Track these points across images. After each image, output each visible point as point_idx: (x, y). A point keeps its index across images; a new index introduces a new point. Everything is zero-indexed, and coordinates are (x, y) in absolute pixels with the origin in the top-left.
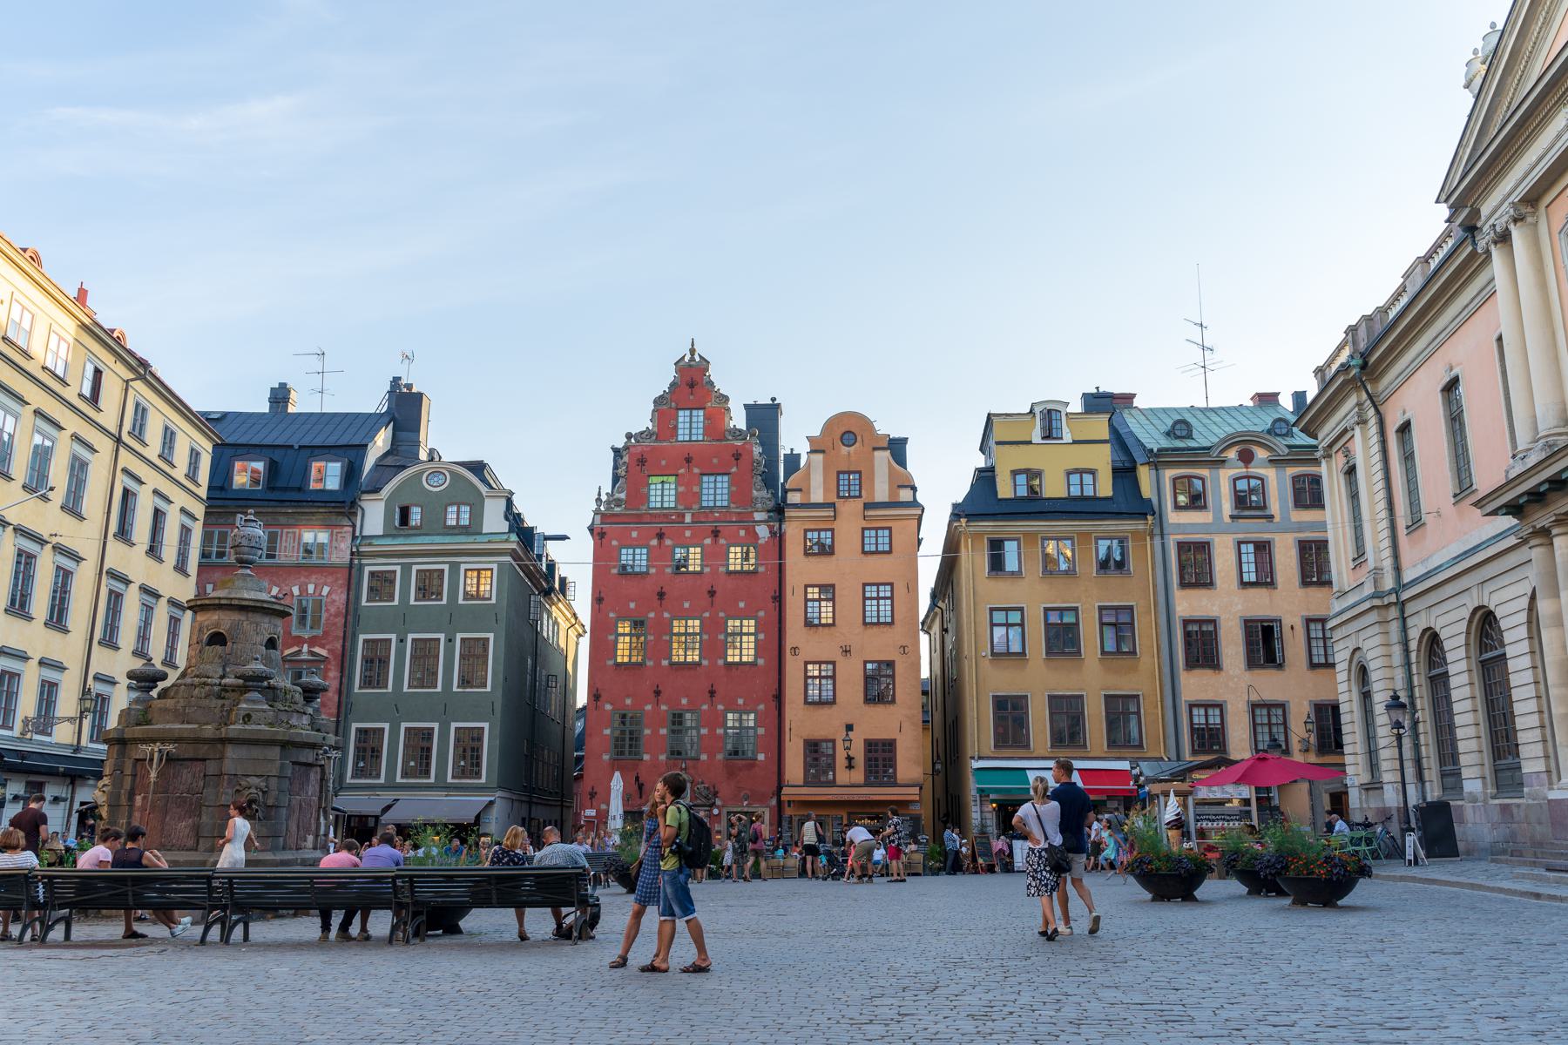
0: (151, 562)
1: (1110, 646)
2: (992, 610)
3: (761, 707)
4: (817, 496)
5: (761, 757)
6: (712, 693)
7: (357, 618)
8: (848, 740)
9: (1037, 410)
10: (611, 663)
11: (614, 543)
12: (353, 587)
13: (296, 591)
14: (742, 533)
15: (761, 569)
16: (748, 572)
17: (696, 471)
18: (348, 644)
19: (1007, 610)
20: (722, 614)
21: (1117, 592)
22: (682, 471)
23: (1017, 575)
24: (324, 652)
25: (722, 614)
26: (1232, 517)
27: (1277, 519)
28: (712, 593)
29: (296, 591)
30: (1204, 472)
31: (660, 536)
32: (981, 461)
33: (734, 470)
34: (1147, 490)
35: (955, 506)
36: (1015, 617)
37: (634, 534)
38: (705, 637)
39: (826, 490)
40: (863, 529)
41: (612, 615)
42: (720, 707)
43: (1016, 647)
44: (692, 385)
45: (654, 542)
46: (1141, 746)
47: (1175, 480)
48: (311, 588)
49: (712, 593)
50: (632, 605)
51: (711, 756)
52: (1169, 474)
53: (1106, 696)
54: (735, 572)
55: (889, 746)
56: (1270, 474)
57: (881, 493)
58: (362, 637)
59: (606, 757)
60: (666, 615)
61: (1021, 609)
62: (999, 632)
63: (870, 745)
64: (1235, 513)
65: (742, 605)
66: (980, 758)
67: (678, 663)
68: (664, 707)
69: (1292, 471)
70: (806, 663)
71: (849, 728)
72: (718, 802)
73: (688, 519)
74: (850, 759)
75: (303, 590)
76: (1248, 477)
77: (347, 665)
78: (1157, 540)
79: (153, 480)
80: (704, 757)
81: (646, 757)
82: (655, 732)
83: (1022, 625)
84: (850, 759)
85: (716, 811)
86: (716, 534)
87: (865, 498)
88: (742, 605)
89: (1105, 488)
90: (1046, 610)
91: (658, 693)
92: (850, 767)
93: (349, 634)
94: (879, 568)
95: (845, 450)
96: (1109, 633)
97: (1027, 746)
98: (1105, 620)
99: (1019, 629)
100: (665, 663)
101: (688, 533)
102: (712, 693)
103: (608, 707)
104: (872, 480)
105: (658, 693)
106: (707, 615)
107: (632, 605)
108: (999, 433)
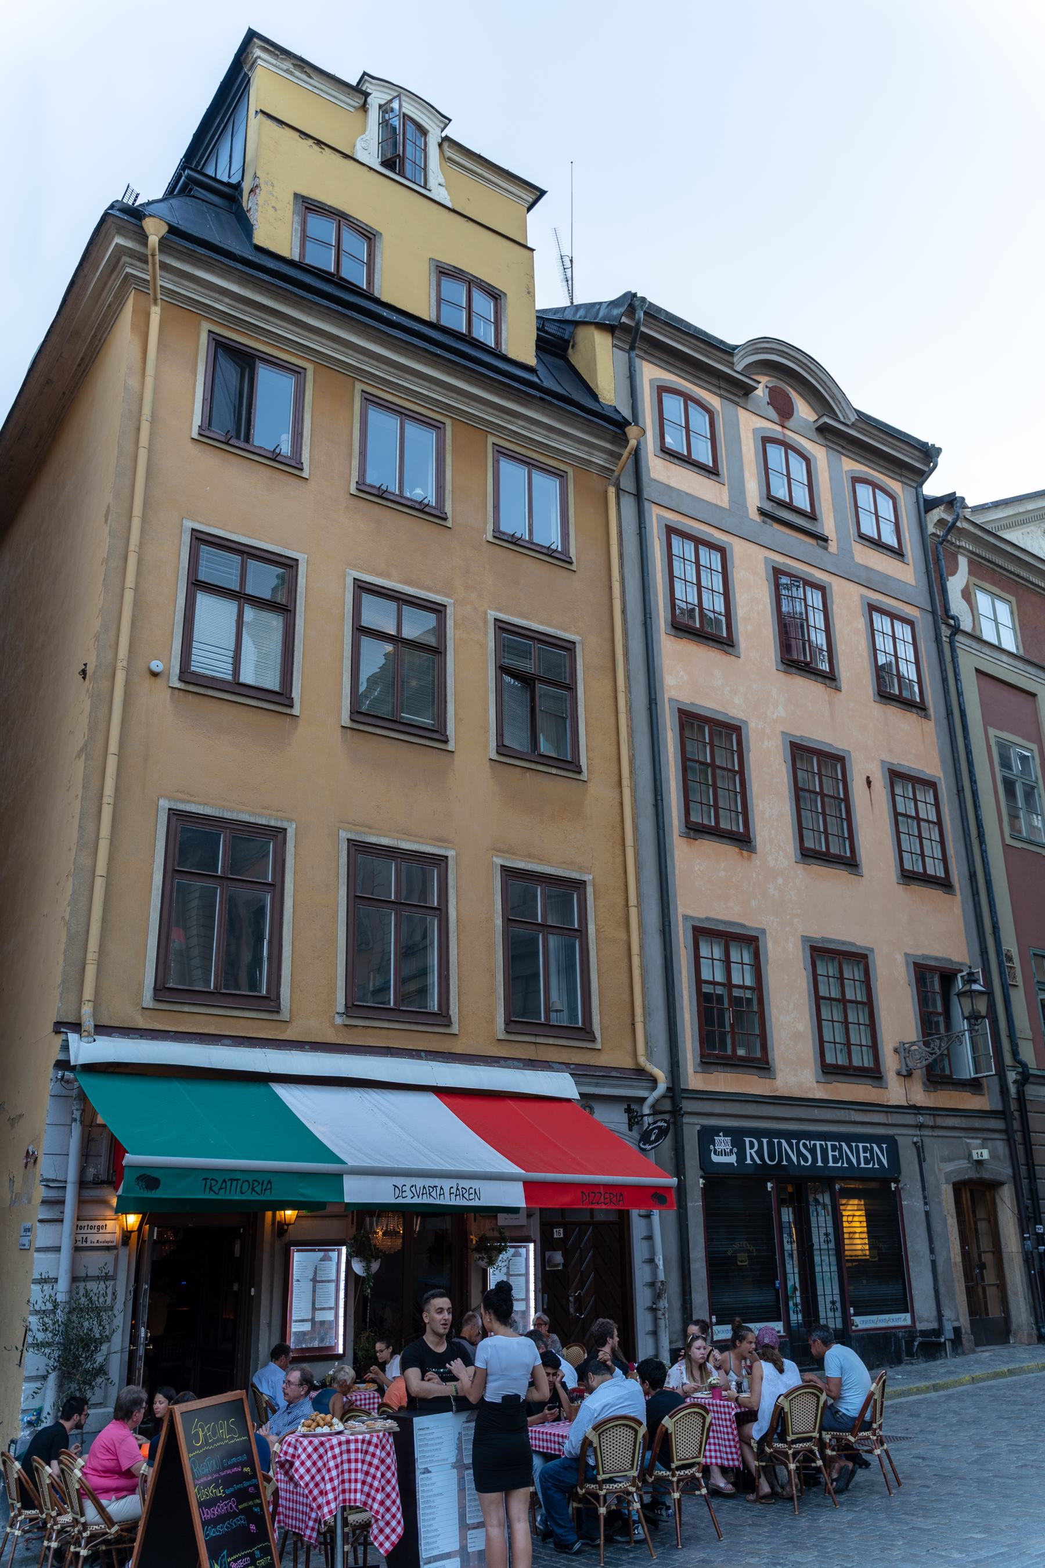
1: (517, 741)
2: (200, 539)
9: (377, 97)
19: (247, 553)
23: (286, 465)
26: (762, 512)
27: (833, 547)
30: (714, 401)
34: (608, 387)
46: (585, 1033)
47: (662, 390)
52: (650, 373)
53: (508, 872)
56: (819, 452)
61: (289, 565)
64: (768, 506)
66: (102, 1029)
69: (850, 465)
76: (788, 446)
78: (628, 504)
89: (520, 345)
90: (362, 588)
97: (271, 1003)
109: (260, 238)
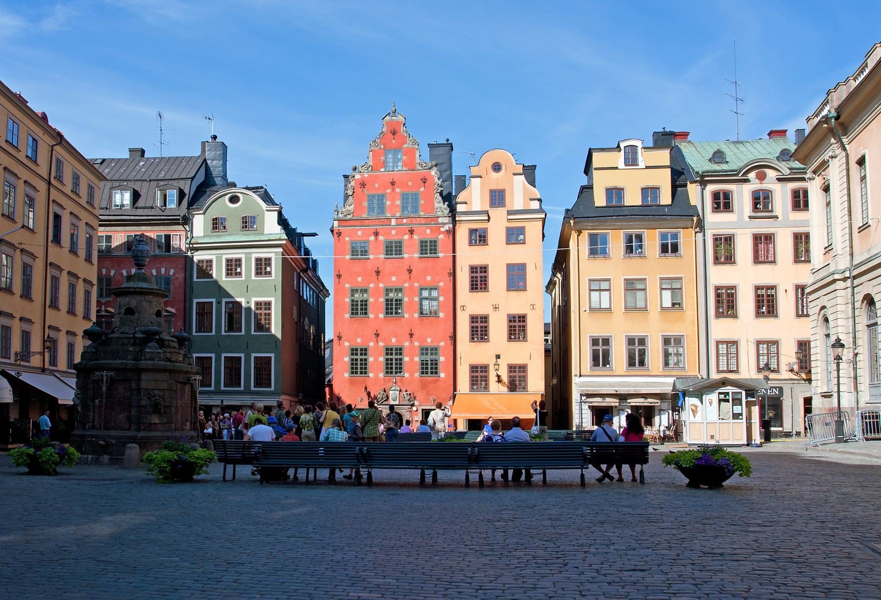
0: (72, 257)
1: (667, 303)
2: (590, 280)
3: (442, 344)
4: (476, 206)
5: (442, 375)
6: (411, 335)
7: (192, 288)
8: (496, 364)
11: (347, 239)
12: (188, 269)
13: (154, 272)
14: (428, 231)
17: (398, 190)
18: (187, 305)
20: (416, 285)
21: (671, 266)
22: (389, 191)
24: (173, 310)
28: (410, 271)
29: (154, 272)
31: (376, 234)
32: (584, 181)
33: (422, 189)
35: (567, 211)
36: (604, 285)
37: (359, 233)
39: (482, 201)
40: (508, 229)
41: (347, 285)
42: (417, 344)
43: (605, 305)
44: (394, 133)
45: (372, 238)
48: (163, 271)
50: (359, 279)
51: (412, 374)
55: (523, 368)
57: (518, 205)
58: (195, 301)
59: (346, 375)
60: (381, 285)
61: (609, 280)
62: (595, 295)
63: (512, 368)
65: (429, 278)
68: (381, 344)
71: (498, 357)
72: (416, 403)
73: (393, 222)
74: (499, 376)
75: (159, 272)
77: (187, 318)
79: (69, 206)
80: (407, 375)
81: (371, 375)
82: (376, 359)
84: (499, 376)
85: (415, 409)
86: (411, 232)
87: (509, 206)
88: (429, 278)
91: (377, 335)
92: (499, 380)
93: (187, 299)
94: (515, 254)
95: (495, 175)
96: (667, 295)
98: (663, 287)
99: (607, 293)
100: (381, 316)
101: (393, 232)
102: (411, 335)
103: (347, 344)
104: (513, 195)
105: (377, 335)
106: (406, 285)
107: (359, 279)
108: (596, 163)
109: (596, 205)
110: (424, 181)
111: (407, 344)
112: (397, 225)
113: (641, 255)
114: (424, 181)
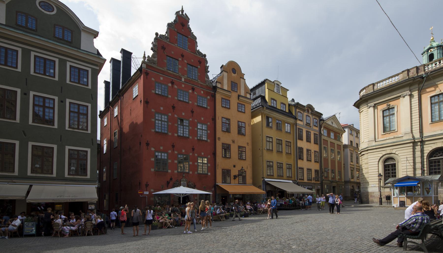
3: (209, 156)
6: (193, 149)
10: (153, 131)
14: (202, 92)
15: (209, 108)
16: (205, 108)
19: (269, 137)
23: (271, 128)
25: (196, 121)
38: (191, 128)
49: (192, 112)
54: (201, 106)
65: (202, 119)
67: (180, 136)
68: (176, 152)
70: (223, 144)
83: (272, 142)
86: (193, 89)
88: (202, 119)
91: (173, 146)
100: (176, 135)
101: (183, 86)
102: (193, 149)
103: (153, 149)
105: (173, 146)
106: (191, 119)
110: (200, 62)
111: (191, 154)
112: (185, 82)
113: (281, 130)
114: (200, 62)
